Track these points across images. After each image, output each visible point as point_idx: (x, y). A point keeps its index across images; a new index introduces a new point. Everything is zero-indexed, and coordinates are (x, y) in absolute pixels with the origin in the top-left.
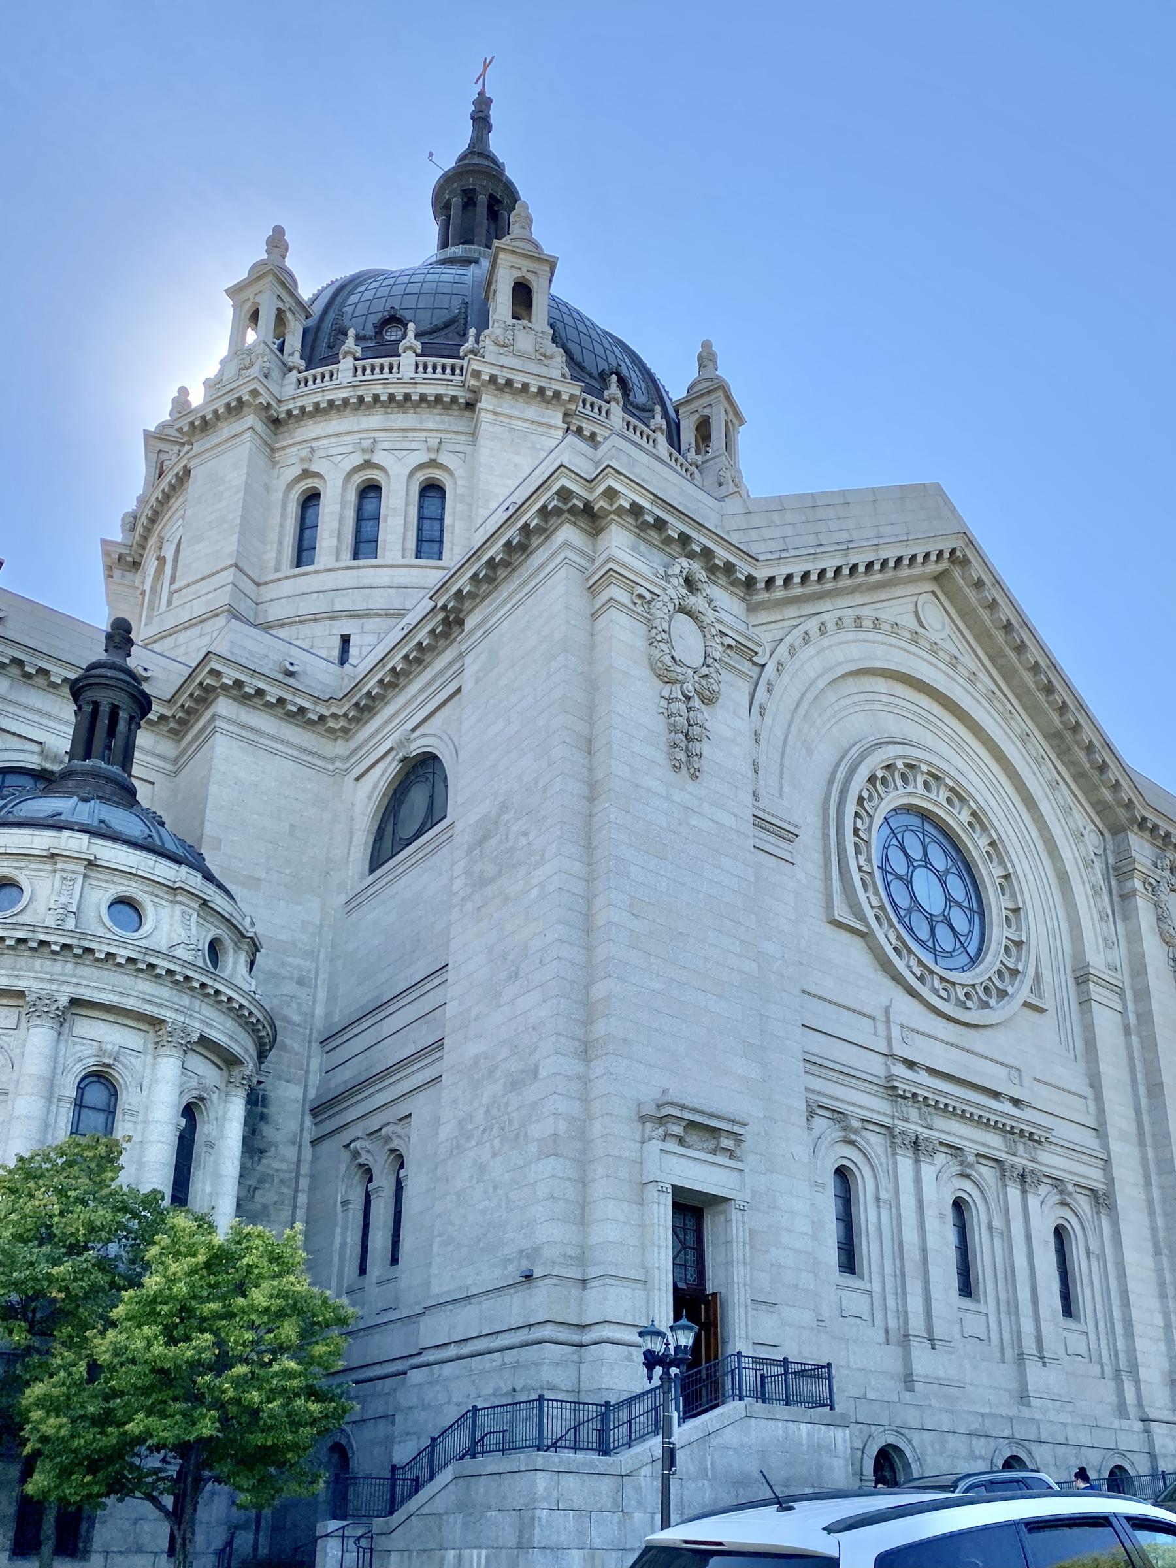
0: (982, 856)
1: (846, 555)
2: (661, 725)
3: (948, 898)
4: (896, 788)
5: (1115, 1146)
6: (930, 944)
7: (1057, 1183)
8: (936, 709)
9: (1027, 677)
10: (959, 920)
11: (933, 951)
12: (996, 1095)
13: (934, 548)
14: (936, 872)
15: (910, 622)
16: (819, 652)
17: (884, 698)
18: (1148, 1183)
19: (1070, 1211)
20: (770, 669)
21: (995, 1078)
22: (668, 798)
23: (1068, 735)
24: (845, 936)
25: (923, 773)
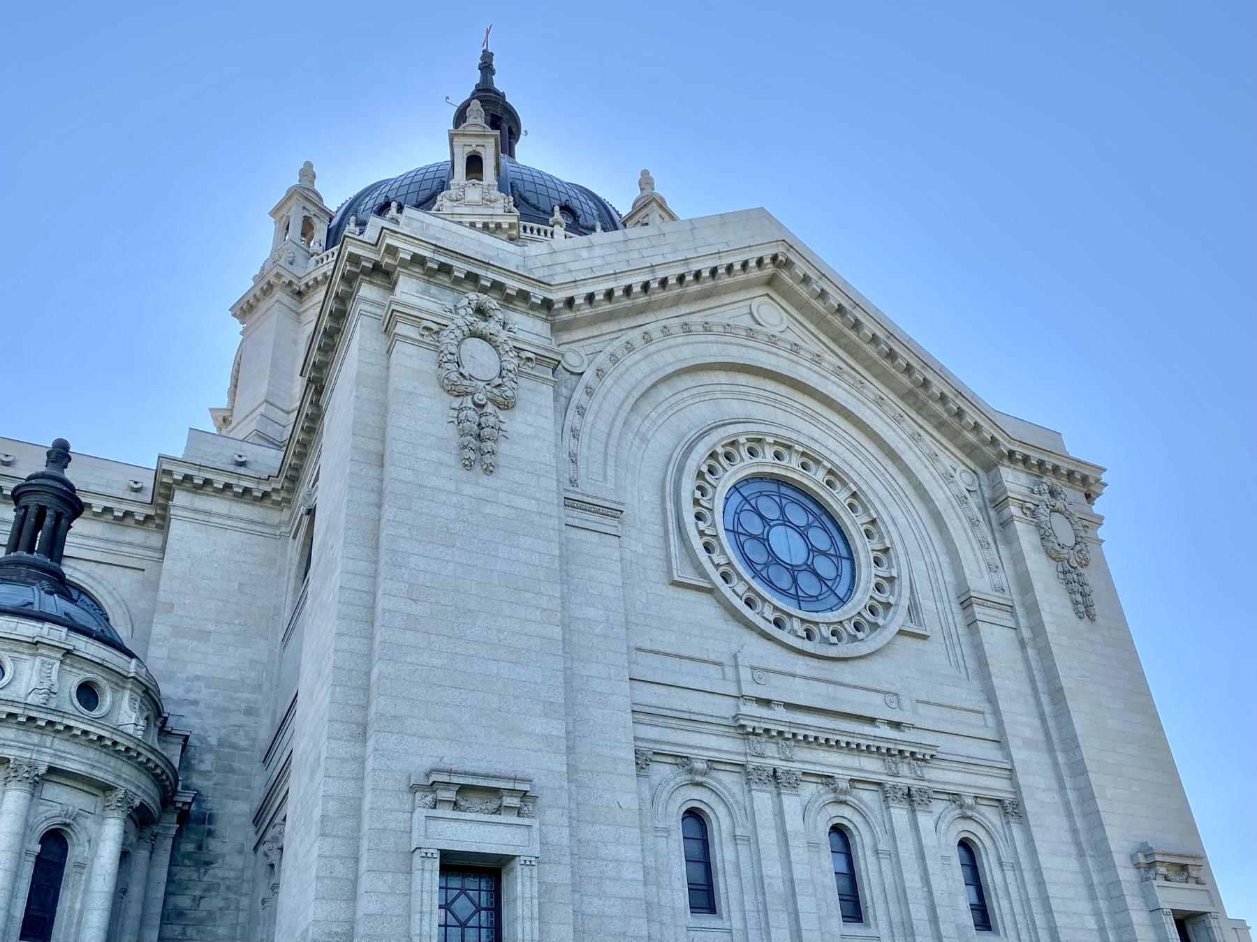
0: (843, 508)
1: (653, 272)
2: (452, 432)
3: (812, 550)
4: (742, 460)
5: (1019, 755)
6: (793, 591)
7: (954, 797)
8: (783, 390)
9: (870, 349)
10: (824, 567)
11: (796, 597)
12: (872, 721)
13: (752, 256)
14: (796, 528)
15: (748, 322)
16: (646, 357)
17: (725, 388)
18: (1062, 787)
19: (975, 824)
20: (589, 375)
21: (871, 705)
22: (458, 492)
23: (921, 393)
24: (691, 595)
25: (769, 444)
